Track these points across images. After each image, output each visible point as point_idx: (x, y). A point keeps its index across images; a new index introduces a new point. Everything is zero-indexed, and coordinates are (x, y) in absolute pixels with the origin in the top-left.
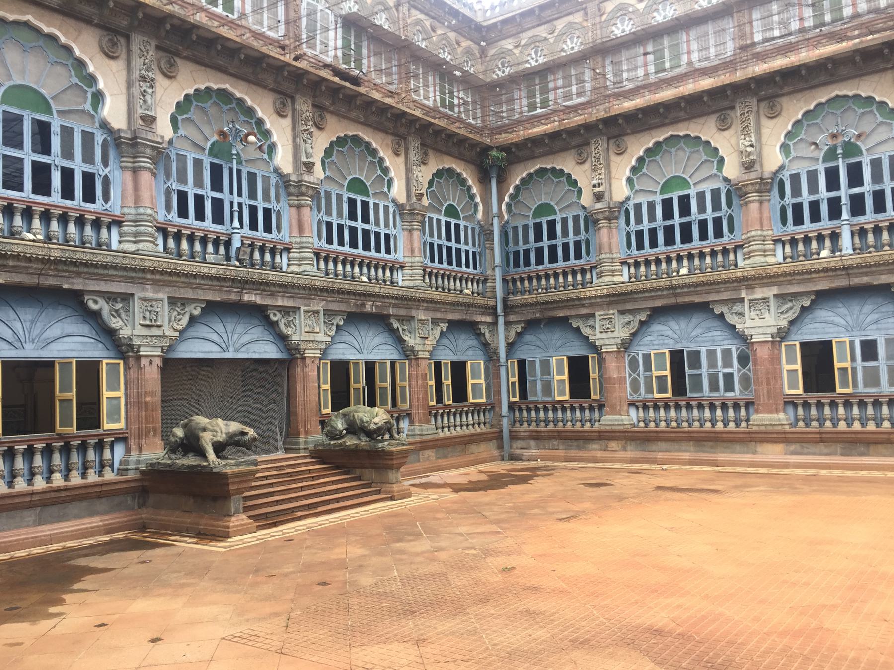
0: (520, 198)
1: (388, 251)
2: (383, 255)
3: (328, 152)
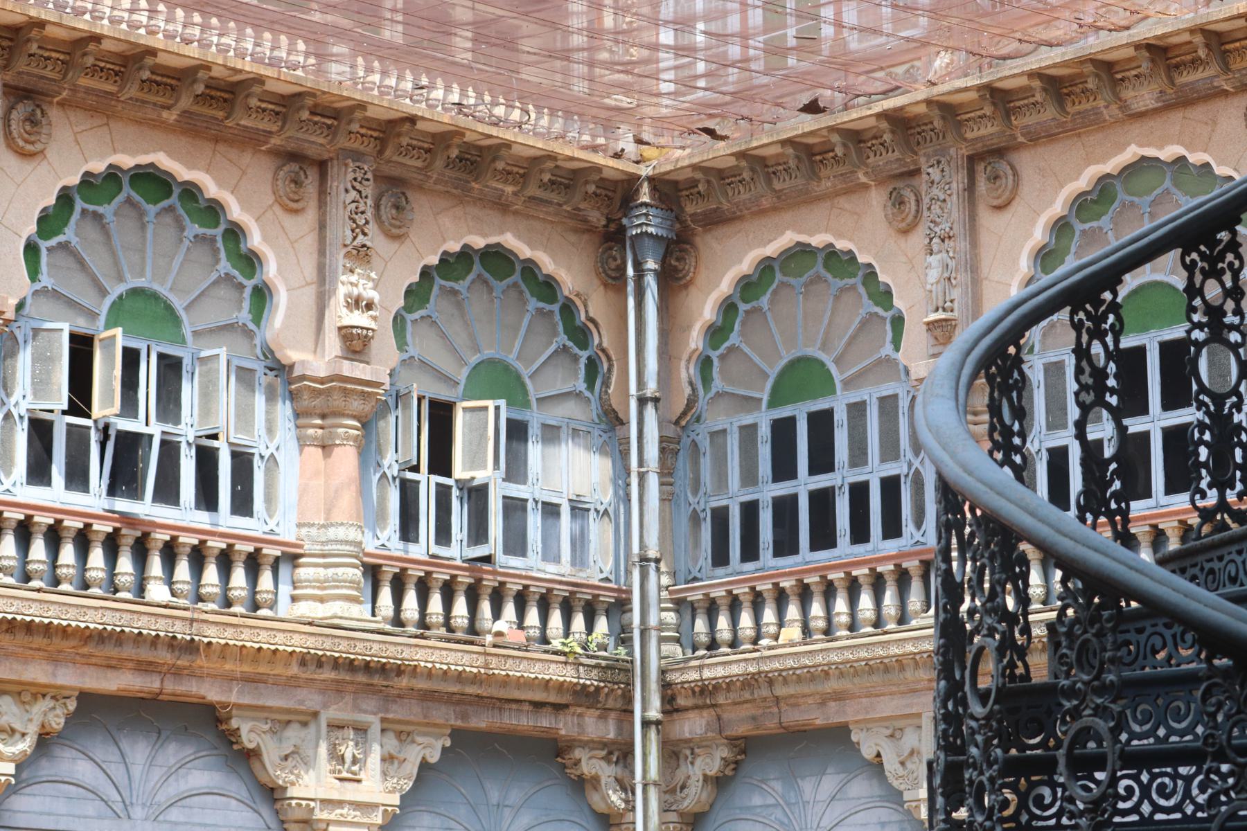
0: (734, 339)
1: (243, 504)
2: (225, 519)
3: (49, 222)
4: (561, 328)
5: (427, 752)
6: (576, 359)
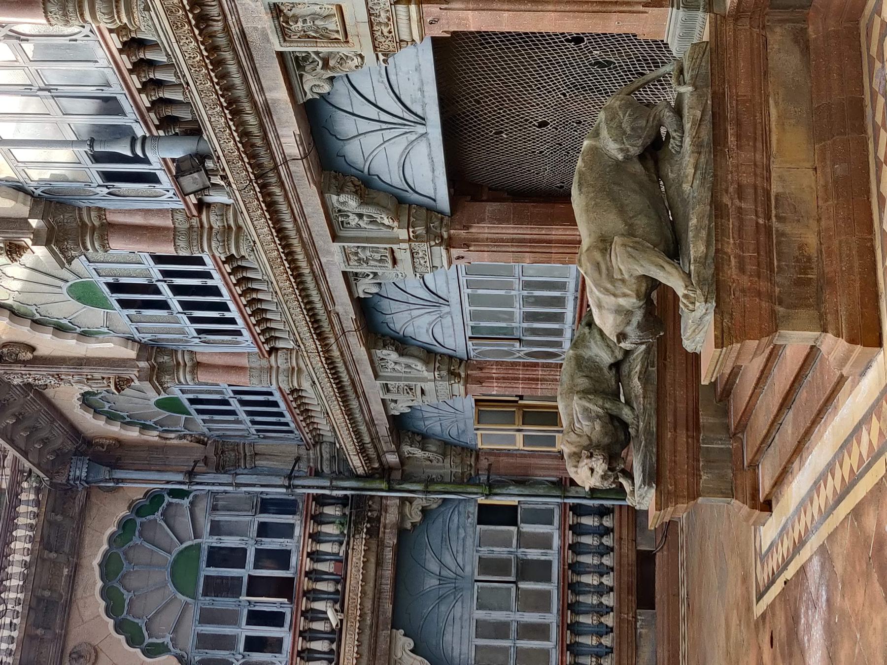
4: (151, 517)
5: (407, 649)
6: (170, 504)
